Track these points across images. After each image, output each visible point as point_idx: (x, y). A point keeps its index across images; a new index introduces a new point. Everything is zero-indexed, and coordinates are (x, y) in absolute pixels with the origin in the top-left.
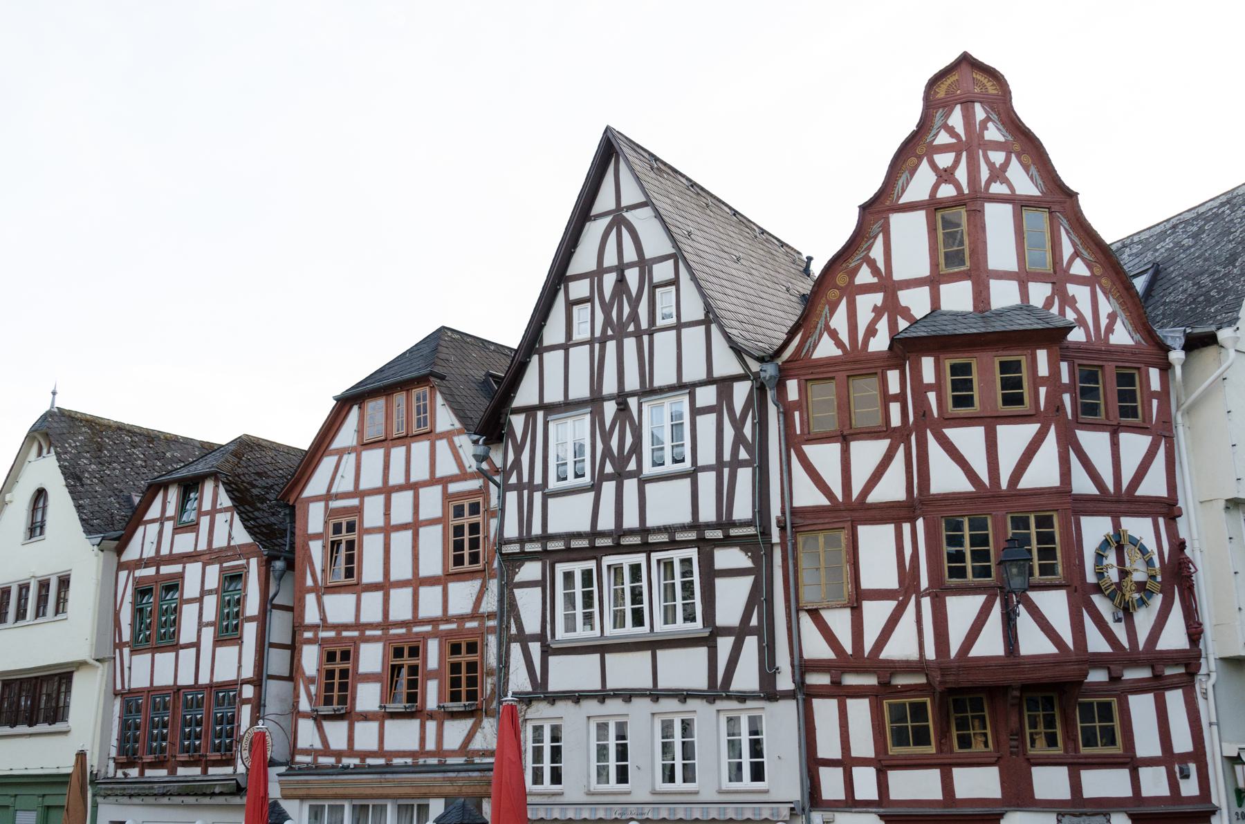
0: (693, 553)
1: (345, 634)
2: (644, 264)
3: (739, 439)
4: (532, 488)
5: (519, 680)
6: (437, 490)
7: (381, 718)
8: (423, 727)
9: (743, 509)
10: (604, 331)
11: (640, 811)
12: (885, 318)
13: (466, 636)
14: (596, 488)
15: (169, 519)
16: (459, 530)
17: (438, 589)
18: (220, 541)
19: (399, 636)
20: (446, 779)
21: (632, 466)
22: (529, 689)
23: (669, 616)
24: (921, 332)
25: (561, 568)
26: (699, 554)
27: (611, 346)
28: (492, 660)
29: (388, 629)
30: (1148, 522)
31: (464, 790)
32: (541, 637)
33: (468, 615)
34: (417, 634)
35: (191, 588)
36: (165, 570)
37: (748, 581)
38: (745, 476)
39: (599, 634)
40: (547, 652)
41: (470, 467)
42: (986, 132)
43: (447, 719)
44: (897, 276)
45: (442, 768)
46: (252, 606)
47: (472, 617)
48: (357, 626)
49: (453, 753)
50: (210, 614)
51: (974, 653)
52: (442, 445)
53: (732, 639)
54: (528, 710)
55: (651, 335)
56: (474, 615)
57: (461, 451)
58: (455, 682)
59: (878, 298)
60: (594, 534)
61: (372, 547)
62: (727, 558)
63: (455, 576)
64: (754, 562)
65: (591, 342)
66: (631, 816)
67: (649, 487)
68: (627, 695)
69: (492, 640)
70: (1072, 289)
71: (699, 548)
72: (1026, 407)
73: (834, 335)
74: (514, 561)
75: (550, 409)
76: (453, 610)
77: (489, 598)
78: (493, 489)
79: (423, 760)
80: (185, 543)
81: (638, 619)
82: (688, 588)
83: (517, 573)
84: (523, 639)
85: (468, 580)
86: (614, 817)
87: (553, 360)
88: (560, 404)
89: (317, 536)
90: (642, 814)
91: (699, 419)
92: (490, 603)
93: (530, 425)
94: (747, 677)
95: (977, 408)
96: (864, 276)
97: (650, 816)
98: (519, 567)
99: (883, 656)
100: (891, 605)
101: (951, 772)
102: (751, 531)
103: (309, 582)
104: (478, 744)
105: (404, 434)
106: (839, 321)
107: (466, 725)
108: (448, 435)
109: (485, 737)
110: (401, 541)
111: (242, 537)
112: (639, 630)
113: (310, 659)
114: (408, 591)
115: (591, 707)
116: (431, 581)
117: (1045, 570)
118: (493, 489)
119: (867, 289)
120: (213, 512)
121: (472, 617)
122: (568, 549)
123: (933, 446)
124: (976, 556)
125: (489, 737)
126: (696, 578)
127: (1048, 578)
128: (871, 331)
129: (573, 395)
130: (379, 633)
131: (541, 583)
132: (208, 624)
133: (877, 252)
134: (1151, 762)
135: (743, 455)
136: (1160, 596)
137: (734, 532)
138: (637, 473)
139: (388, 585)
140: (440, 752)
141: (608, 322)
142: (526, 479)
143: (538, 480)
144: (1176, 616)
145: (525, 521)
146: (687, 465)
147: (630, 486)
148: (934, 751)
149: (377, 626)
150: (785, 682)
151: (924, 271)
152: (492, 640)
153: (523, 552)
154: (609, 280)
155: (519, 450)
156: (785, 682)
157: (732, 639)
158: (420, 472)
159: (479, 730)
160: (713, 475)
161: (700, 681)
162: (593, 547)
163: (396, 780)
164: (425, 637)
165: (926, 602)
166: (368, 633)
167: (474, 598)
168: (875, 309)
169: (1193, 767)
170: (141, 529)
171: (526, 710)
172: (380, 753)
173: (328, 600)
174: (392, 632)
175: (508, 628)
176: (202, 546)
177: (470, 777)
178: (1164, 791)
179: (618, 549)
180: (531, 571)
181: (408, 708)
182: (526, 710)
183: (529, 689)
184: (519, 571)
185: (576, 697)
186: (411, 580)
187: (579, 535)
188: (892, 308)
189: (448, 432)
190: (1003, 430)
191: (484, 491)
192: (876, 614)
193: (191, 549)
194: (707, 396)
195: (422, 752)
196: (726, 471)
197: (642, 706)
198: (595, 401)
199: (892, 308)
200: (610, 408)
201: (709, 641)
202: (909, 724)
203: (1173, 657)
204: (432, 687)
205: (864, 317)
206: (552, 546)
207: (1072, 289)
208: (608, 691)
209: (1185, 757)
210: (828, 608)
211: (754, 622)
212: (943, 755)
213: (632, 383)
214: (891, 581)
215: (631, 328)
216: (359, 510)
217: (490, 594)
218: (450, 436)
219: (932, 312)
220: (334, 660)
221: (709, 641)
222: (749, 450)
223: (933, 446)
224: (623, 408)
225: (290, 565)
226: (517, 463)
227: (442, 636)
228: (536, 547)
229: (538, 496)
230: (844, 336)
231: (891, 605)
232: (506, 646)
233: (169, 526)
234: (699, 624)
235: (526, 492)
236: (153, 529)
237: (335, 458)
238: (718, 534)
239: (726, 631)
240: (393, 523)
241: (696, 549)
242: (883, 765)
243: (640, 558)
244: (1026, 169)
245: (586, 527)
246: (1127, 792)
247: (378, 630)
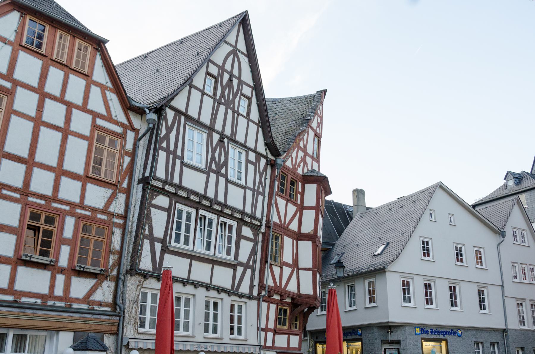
4: (175, 157)
7: (14, 264)
8: (53, 279)
10: (220, 98)
11: (206, 347)
13: (97, 223)
17: (78, 184)
20: (82, 319)
22: (151, 270)
25: (179, 206)
26: (237, 225)
29: (28, 196)
31: (93, 327)
32: (163, 241)
33: (99, 209)
39: (191, 249)
40: (165, 250)
41: (116, 116)
43: (74, 276)
45: (68, 309)
47: (102, 212)
49: (77, 300)
54: (145, 282)
57: (110, 102)
63: (94, 180)
66: (201, 349)
68: (196, 285)
71: (238, 222)
75: (188, 118)
76: (88, 202)
77: (117, 204)
79: (53, 302)
83: (154, 199)
84: (153, 240)
85: (103, 187)
86: (194, 349)
88: (195, 120)
90: (207, 348)
97: (210, 349)
98: (156, 196)
102: (258, 223)
104: (98, 296)
107: (90, 282)
109: (104, 294)
121: (102, 212)
122: (188, 198)
125: (106, 293)
130: (17, 196)
138: (226, 176)
139: (31, 162)
140: (66, 298)
141: (223, 95)
142: (172, 148)
148: (287, 328)
149: (16, 190)
153: (163, 189)
155: (169, 130)
156: (255, 293)
159: (100, 288)
162: (199, 203)
163: (35, 315)
166: (4, 192)
167: (106, 200)
171: (144, 281)
174: (31, 199)
177: (101, 318)
179: (209, 209)
180: (162, 201)
181: (53, 262)
182: (144, 281)
183: (151, 270)
184: (156, 198)
186: (55, 168)
187: (196, 194)
189: (102, 84)
191: (123, 136)
192: (287, 271)
195: (51, 296)
197: (201, 292)
204: (65, 250)
208: (190, 280)
210: (275, 265)
212: (289, 330)
215: (232, 106)
217: (118, 202)
218: (103, 88)
221: (233, 266)
227: (79, 217)
228: (172, 190)
229: (178, 162)
232: (142, 240)
234: (232, 257)
235: (171, 156)
239: (241, 264)
241: (236, 222)
242: (275, 332)
247: (17, 193)
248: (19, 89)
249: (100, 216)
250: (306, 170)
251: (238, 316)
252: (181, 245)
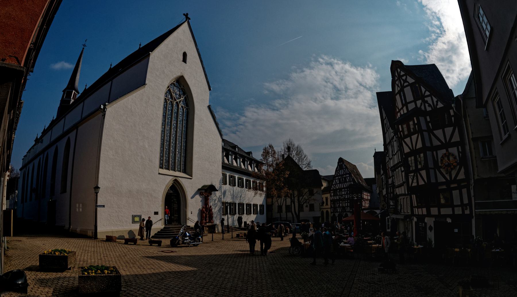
30: (456, 148)
70: (426, 99)
134: (458, 206)
144: (463, 170)
169: (468, 207)
178: (460, 212)
203: (462, 180)
207: (426, 99)
209: (466, 205)
246: (451, 213)
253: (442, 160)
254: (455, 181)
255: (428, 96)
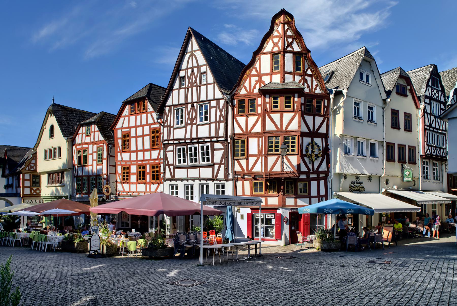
0: (209, 144)
1: (127, 163)
2: (198, 67)
3: (221, 115)
4: (171, 127)
5: (168, 175)
6: (148, 127)
9: (221, 133)
10: (188, 85)
12: (258, 84)
14: (186, 127)
15: (84, 133)
16: (153, 137)
18: (96, 139)
19: (157, 162)
21: (195, 122)
23: (203, 160)
24: (267, 88)
25: (178, 147)
27: (190, 89)
28: (162, 171)
32: (173, 165)
34: (144, 163)
35: (90, 151)
36: (84, 146)
37: (222, 152)
38: (222, 125)
42: (287, 33)
44: (262, 72)
46: (105, 156)
48: (130, 161)
50: (95, 158)
51: (274, 170)
52: (149, 115)
53: (218, 166)
55: (200, 87)
56: (158, 159)
58: (154, 175)
59: (257, 78)
60: (185, 139)
61: (133, 141)
62: (218, 146)
64: (224, 147)
65: (185, 88)
67: (199, 127)
68: (194, 179)
69: (162, 165)
72: (292, 109)
73: (245, 88)
74: (166, 146)
75: (175, 106)
76: (153, 158)
78: (162, 127)
80: (88, 140)
81: (196, 161)
82: (208, 154)
84: (169, 165)
87: (175, 93)
89: (119, 138)
91: (211, 109)
92: (161, 156)
93: (170, 110)
94: (221, 175)
95: (279, 109)
96: (254, 72)
99: (253, 171)
100: (255, 158)
101: (267, 199)
102: (223, 139)
103: (118, 150)
105: (140, 112)
106: (247, 84)
108: (151, 113)
110: (140, 140)
111: (102, 138)
112: (184, 164)
113: (119, 169)
114: (142, 153)
115: (185, 182)
116: (147, 150)
117: (293, 150)
118: (162, 127)
119: (254, 76)
120: (94, 132)
122: (180, 143)
123: (267, 118)
124: (276, 147)
126: (210, 151)
127: (293, 153)
128: (255, 87)
129: (180, 103)
131: (173, 151)
132: (95, 160)
133: (257, 65)
135: (222, 119)
136: (321, 158)
137: (219, 139)
142: (169, 124)
143: (172, 125)
145: (169, 135)
146: (208, 122)
147: (194, 127)
150: (230, 177)
151: (269, 71)
152: (162, 165)
154: (190, 71)
156: (230, 177)
157: (218, 166)
158: (144, 122)
160: (214, 124)
161: (210, 176)
164: (146, 164)
165: (263, 158)
168: (256, 81)
170: (78, 135)
172: (136, 192)
173: (123, 154)
175: (165, 163)
176: (92, 140)
180: (170, 148)
185: (182, 180)
188: (260, 81)
190: (285, 115)
192: (252, 160)
193: (89, 141)
194: (213, 103)
196: (218, 123)
198: (186, 104)
199: (260, 81)
200: (190, 106)
201: (213, 166)
202: (289, 185)
205: (253, 83)
206: (176, 142)
211: (223, 162)
213: (195, 100)
214: (256, 153)
216: (130, 132)
219: (270, 83)
220: (125, 169)
221: (213, 166)
222: (223, 118)
223: (267, 118)
224: (193, 106)
225: (114, 146)
226: (167, 120)
229: (172, 129)
230: (248, 88)
231: (255, 158)
233: (84, 135)
234: (210, 162)
235: (169, 128)
236: (80, 136)
237: (123, 118)
238: (215, 139)
239: (217, 164)
240: (138, 135)
243: (197, 145)
244: (297, 43)
245: (183, 137)
248: (132, 129)
249: (156, 161)
250: (262, 85)
251: (222, 191)
252: (182, 164)
253: (307, 148)
254: (317, 172)
255: (309, 75)
